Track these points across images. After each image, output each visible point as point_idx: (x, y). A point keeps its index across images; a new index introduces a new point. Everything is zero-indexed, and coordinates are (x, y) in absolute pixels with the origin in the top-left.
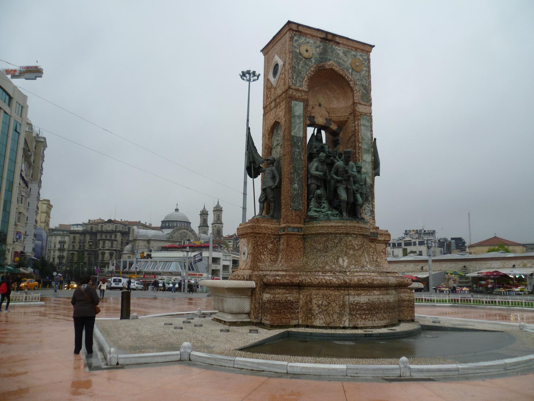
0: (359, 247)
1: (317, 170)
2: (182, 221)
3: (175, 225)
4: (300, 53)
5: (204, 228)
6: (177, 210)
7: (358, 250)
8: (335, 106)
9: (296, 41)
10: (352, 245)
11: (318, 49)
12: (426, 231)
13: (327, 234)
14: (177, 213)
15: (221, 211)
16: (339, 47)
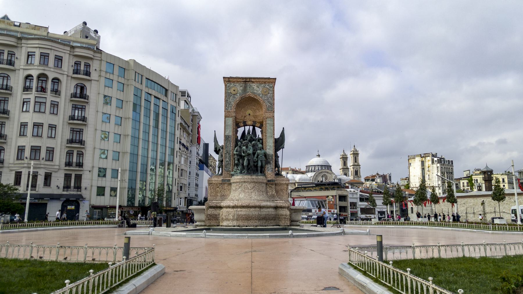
0: (251, 188)
1: (237, 151)
5: (345, 170)
7: (251, 189)
8: (258, 114)
9: (228, 86)
10: (247, 187)
11: (241, 88)
13: (236, 182)
15: (358, 154)
16: (254, 83)
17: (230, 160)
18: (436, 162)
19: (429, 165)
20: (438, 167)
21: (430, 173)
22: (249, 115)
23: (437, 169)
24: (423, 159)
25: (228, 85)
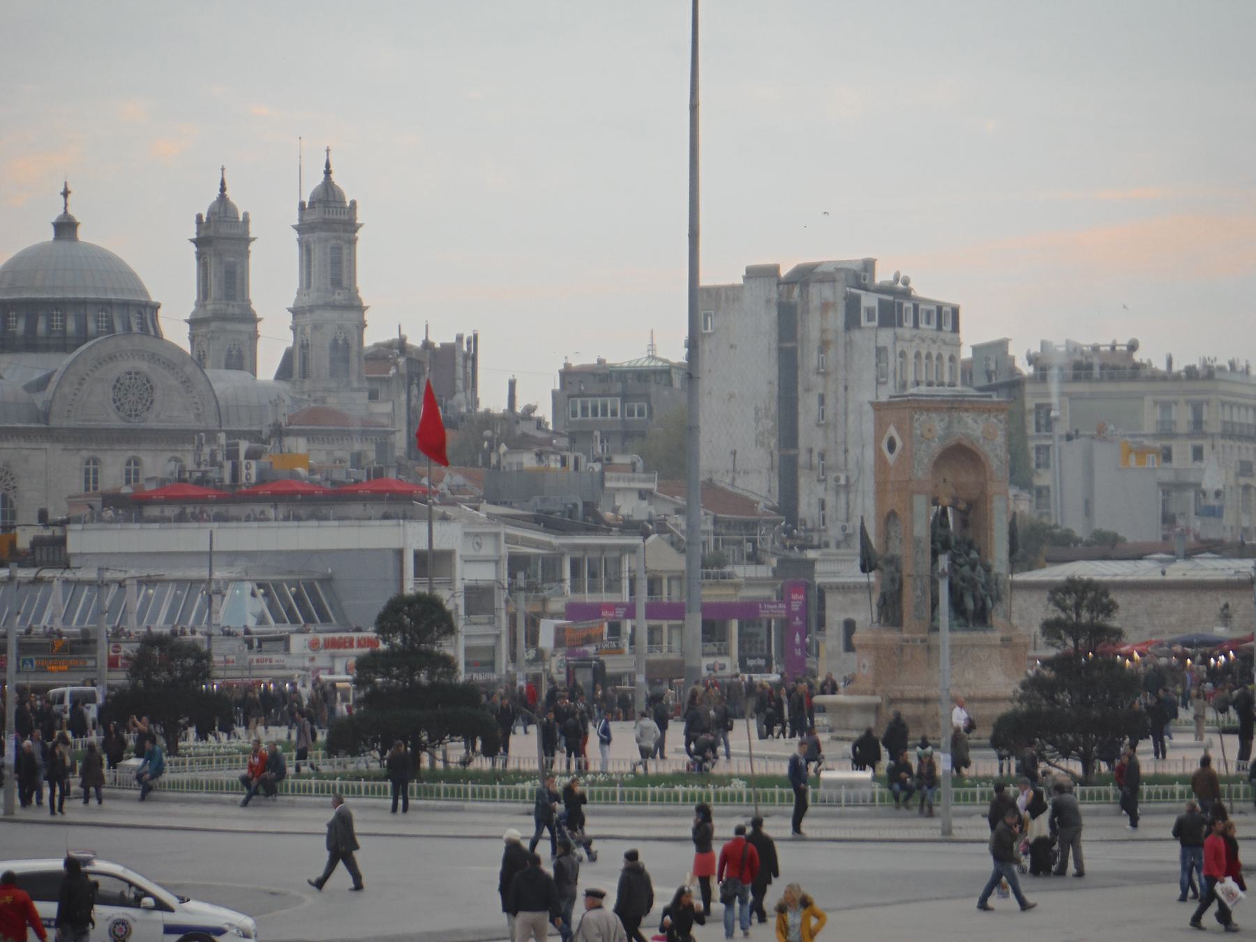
2: (109, 304)
3: (71, 326)
4: (922, 436)
5: (230, 326)
6: (66, 227)
9: (917, 420)
11: (942, 424)
14: (65, 245)
17: (924, 593)
18: (870, 319)
19: (830, 336)
20: (880, 352)
22: (945, 481)
23: (873, 360)
24: (790, 292)
25: (916, 416)
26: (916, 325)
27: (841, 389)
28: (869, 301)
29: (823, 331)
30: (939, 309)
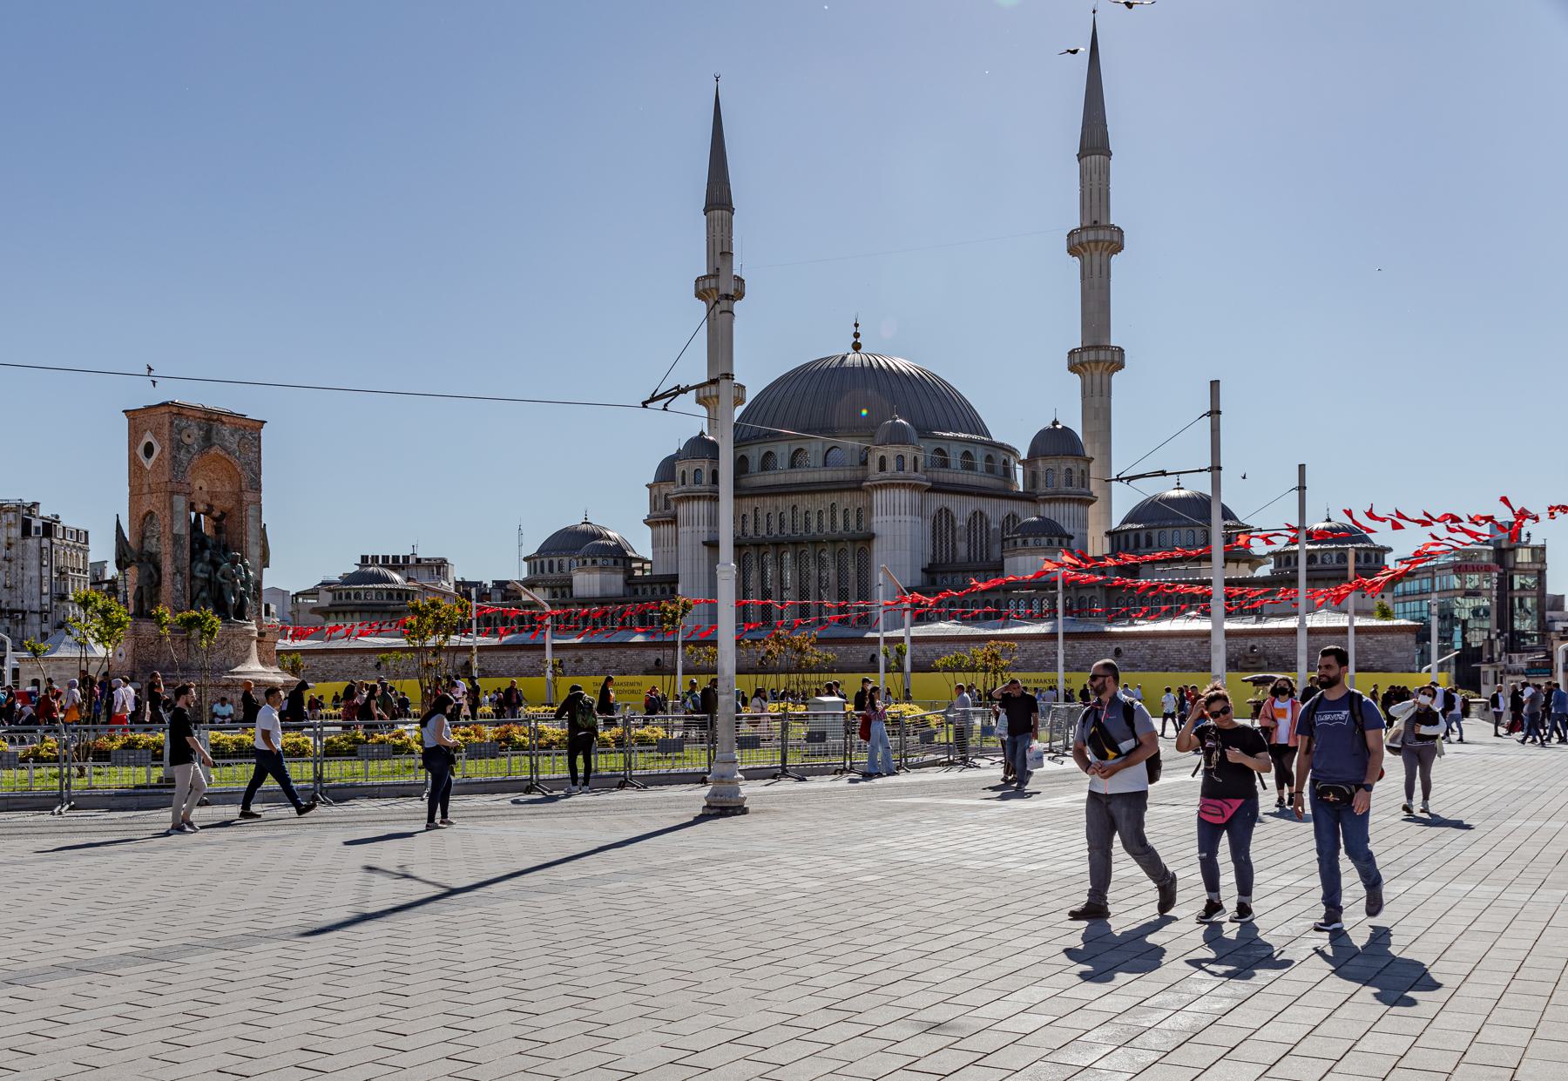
12: (423, 562)
19: (12, 541)
21: (14, 567)
22: (201, 488)
26: (64, 538)
27: (20, 570)
28: (36, 523)
29: (8, 538)
30: (78, 531)
